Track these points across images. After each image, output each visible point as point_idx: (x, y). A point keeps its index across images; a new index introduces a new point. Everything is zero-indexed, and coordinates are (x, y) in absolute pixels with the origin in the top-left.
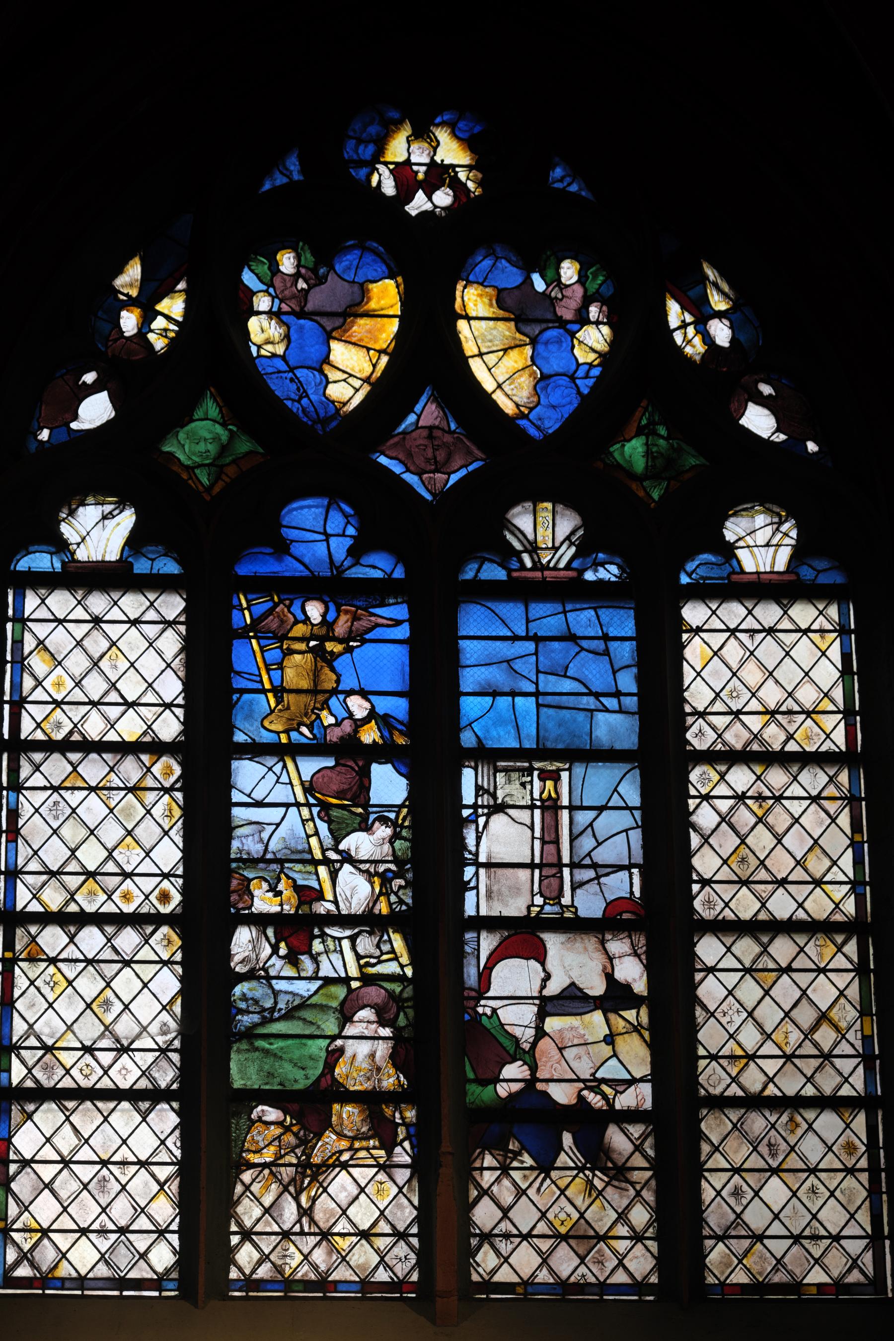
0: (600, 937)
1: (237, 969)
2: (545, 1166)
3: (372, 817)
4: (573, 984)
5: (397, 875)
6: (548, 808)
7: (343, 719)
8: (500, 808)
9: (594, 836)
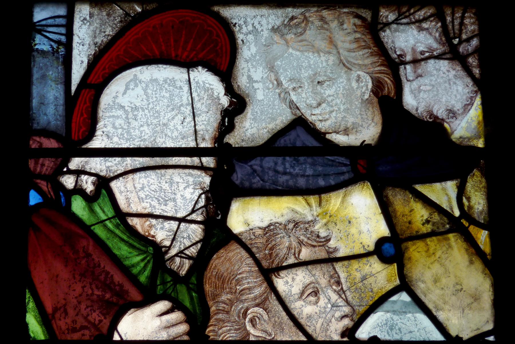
0: (367, 15)
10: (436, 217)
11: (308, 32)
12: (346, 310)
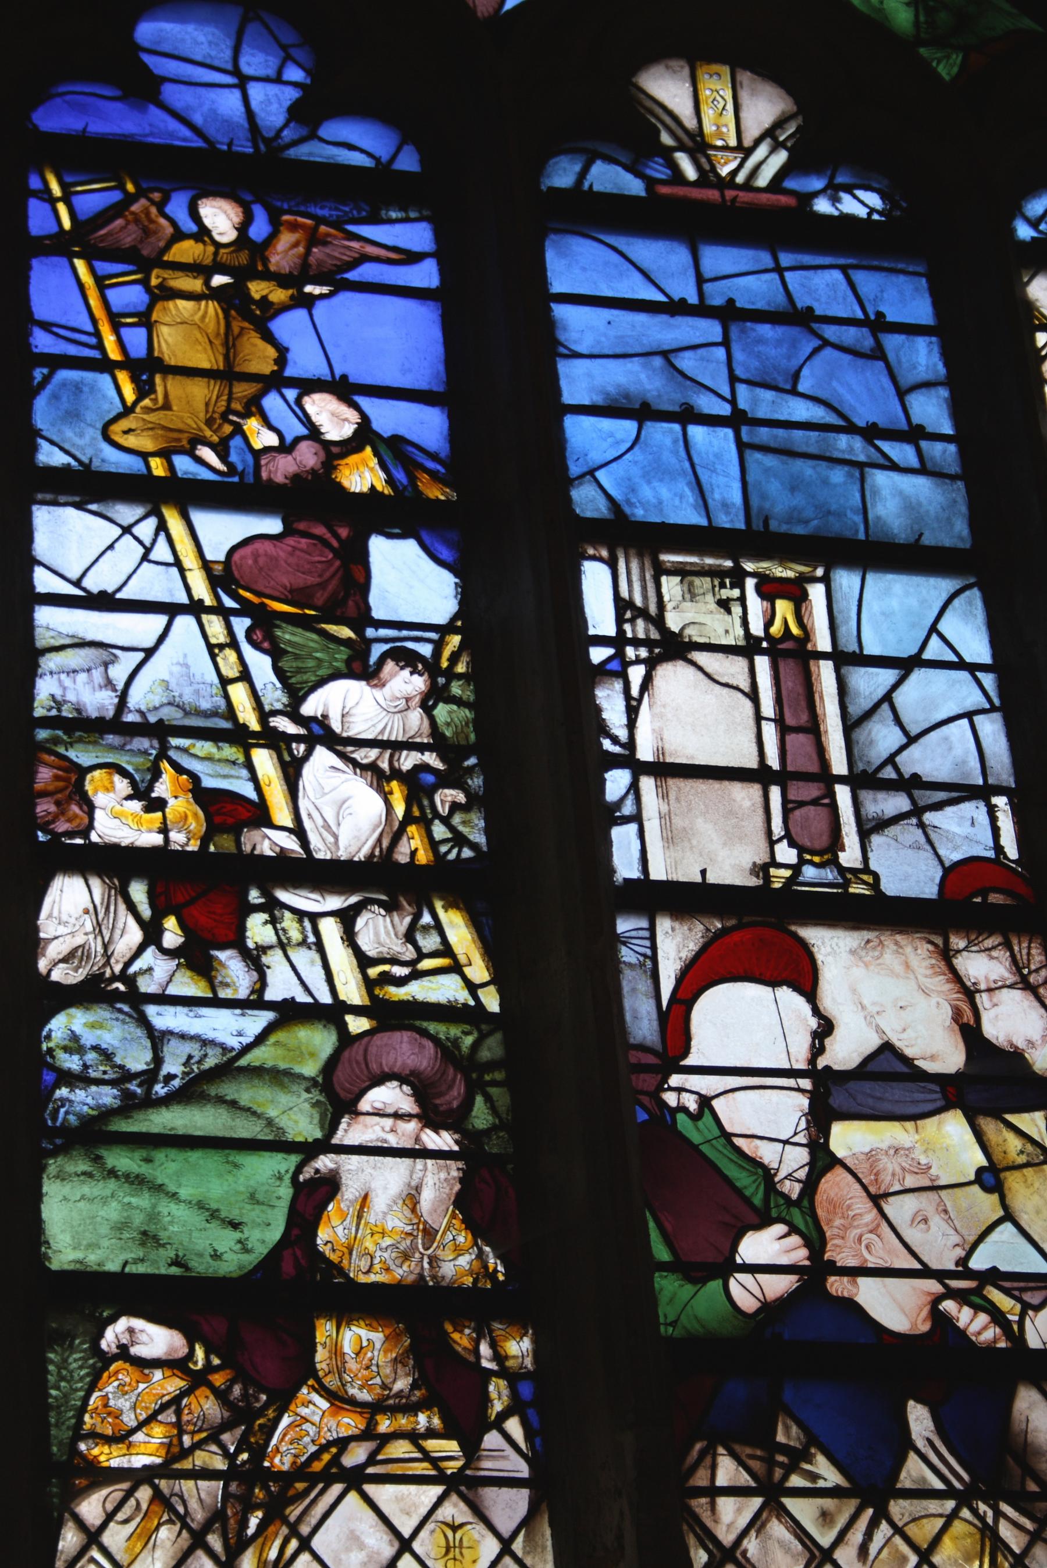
0: (939, 941)
1: (56, 976)
2: (873, 1488)
3: (377, 650)
4: (887, 1048)
5: (445, 780)
6: (787, 654)
7: (298, 440)
8: (674, 647)
9: (898, 721)
10: (1029, 1148)
11: (885, 956)
12: (956, 1239)
